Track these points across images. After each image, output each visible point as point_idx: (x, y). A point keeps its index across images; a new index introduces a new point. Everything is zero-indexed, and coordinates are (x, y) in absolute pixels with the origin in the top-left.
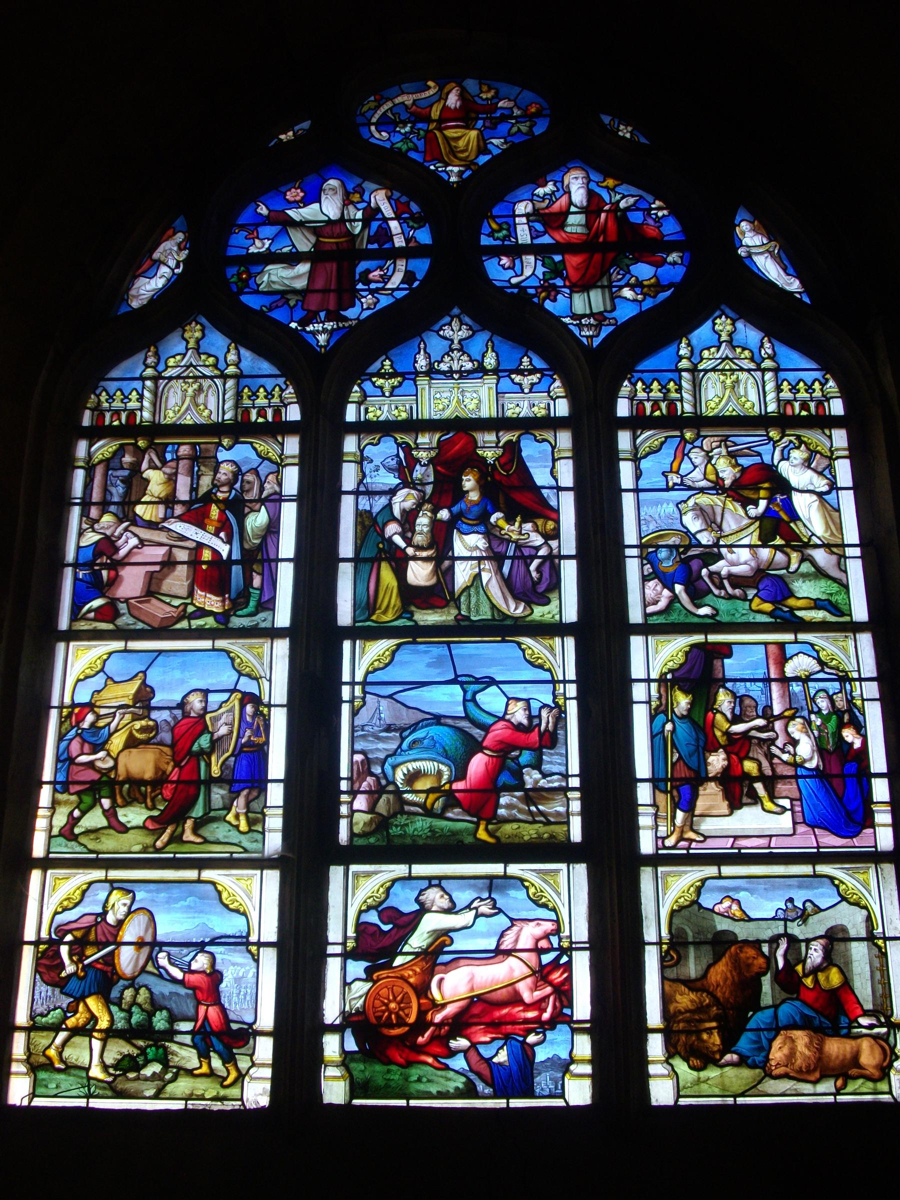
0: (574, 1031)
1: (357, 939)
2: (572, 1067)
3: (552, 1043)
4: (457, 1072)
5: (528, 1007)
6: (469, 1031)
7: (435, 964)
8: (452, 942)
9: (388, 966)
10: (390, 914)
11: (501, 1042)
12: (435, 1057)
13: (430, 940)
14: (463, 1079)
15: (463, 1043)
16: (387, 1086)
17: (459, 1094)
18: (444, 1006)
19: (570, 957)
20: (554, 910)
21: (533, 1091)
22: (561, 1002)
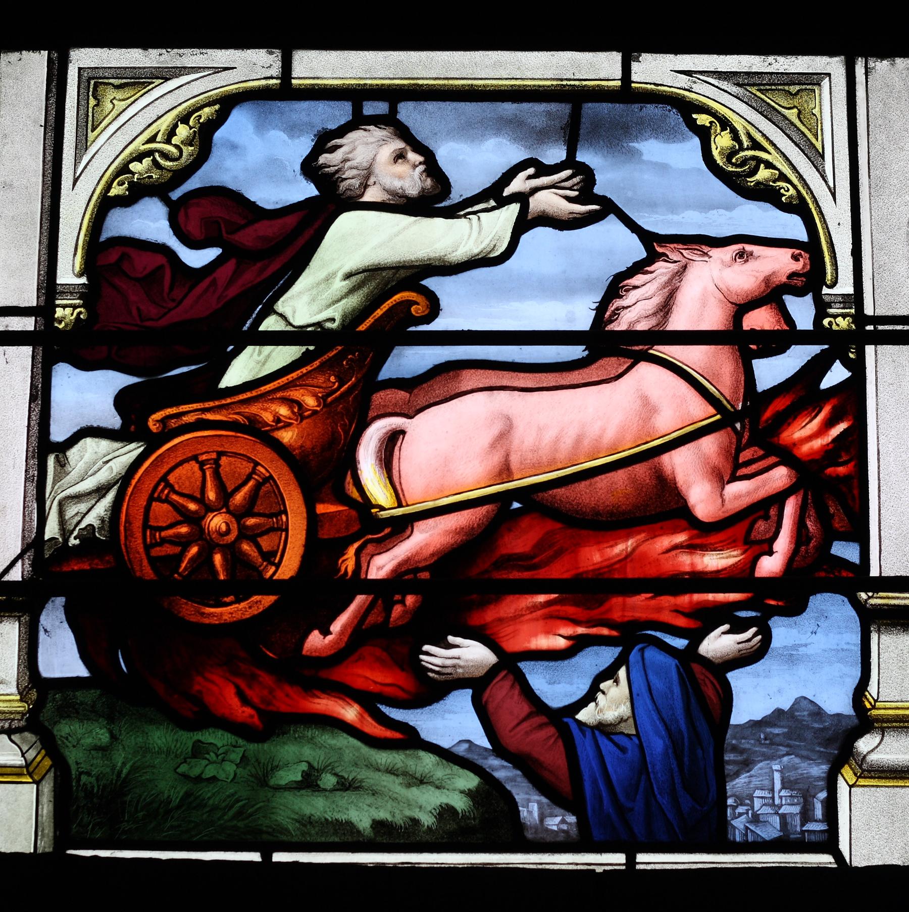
0: (871, 620)
1: (88, 296)
2: (864, 744)
3: (792, 658)
4: (446, 755)
5: (706, 534)
6: (490, 615)
7: (371, 384)
8: (434, 309)
9: (205, 386)
10: (216, 213)
11: (607, 655)
12: (368, 701)
13: (353, 301)
14: (470, 781)
15: (473, 654)
16: (189, 802)
17: (452, 832)
18: (402, 526)
19: (858, 368)
20: (800, 207)
21: (723, 824)
22: (824, 519)
